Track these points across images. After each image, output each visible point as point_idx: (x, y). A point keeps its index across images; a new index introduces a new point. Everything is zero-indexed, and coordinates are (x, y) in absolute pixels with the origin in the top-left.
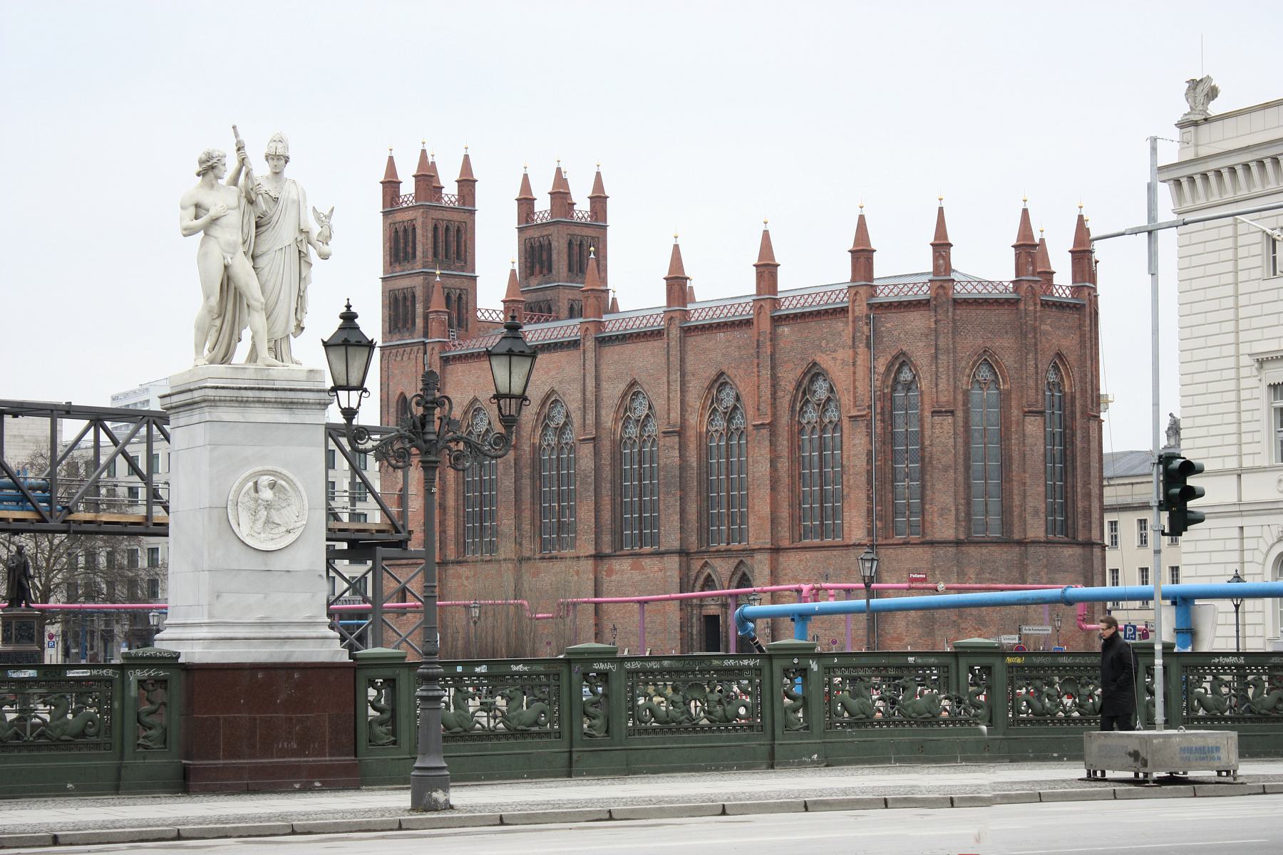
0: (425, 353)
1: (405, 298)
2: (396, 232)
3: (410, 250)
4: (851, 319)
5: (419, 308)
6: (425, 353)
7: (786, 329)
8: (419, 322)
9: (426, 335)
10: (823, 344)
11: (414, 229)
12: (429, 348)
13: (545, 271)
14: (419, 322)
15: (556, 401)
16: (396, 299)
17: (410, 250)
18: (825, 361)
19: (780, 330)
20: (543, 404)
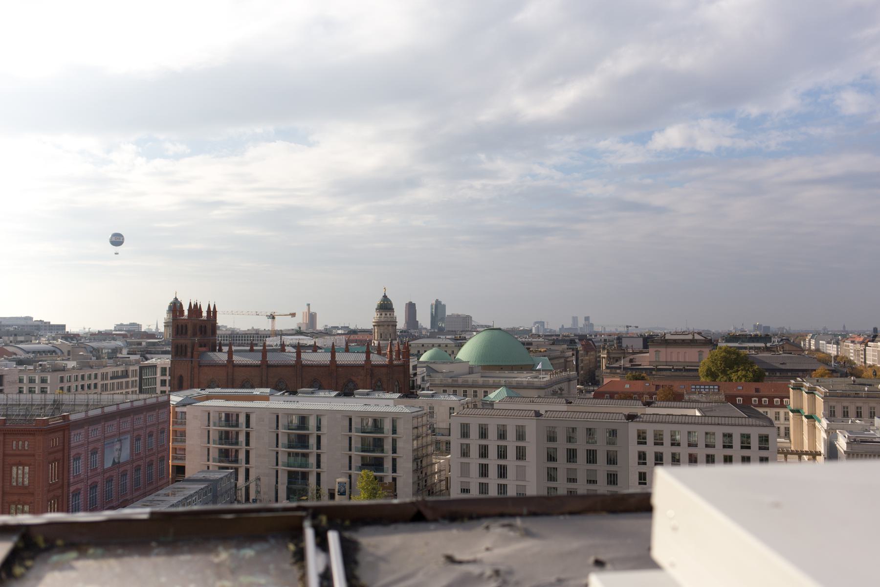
0: (192, 363)
1: (182, 346)
2: (178, 325)
3: (184, 331)
4: (365, 368)
5: (189, 350)
6: (192, 363)
7: (340, 369)
8: (189, 354)
9: (192, 357)
10: (354, 374)
11: (186, 326)
12: (193, 362)
13: (203, 334)
14: (189, 354)
15: (247, 381)
16: (177, 345)
17: (184, 331)
18: (354, 378)
19: (338, 369)
20: (242, 382)
